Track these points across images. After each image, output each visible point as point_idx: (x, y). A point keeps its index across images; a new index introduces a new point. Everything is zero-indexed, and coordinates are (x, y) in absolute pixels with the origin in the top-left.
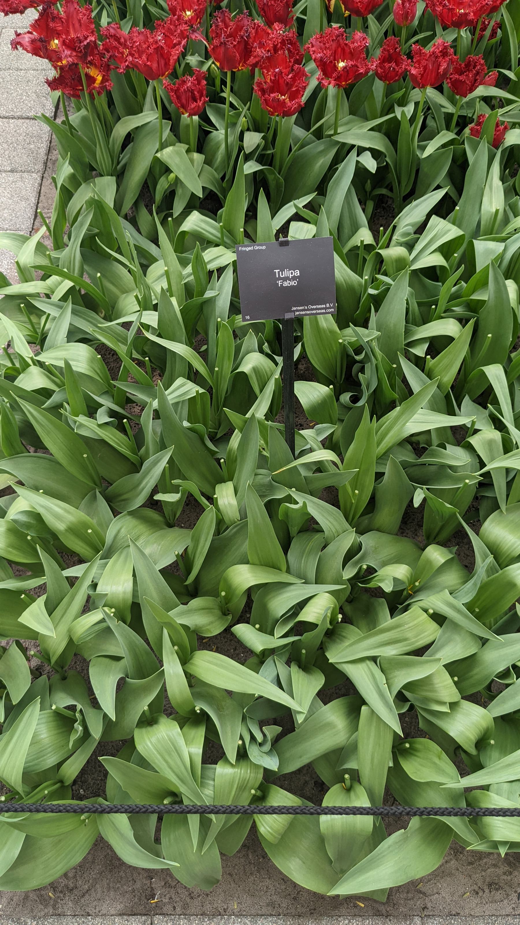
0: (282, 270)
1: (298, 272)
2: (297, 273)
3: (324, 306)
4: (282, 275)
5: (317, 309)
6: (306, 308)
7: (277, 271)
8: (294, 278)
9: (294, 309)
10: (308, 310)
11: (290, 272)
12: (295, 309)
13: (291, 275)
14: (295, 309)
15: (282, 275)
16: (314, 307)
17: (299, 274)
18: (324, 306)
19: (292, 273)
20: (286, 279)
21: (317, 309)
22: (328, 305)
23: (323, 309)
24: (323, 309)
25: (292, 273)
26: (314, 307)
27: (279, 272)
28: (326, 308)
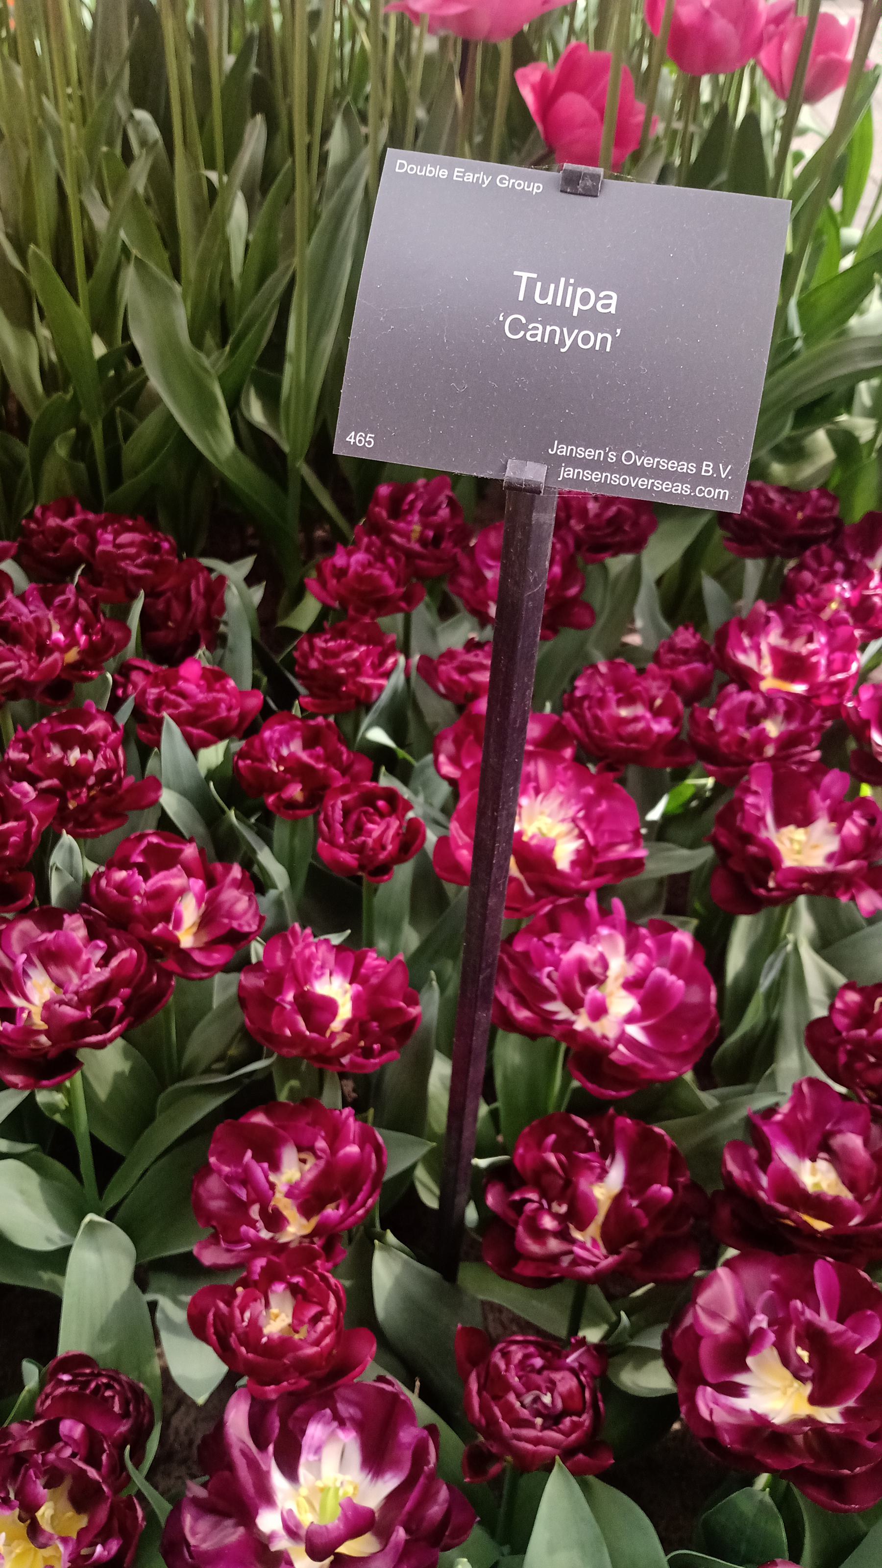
0: (548, 278)
4: (544, 295)
5: (656, 473)
6: (612, 457)
7: (525, 275)
9: (562, 450)
10: (618, 468)
13: (578, 305)
15: (544, 295)
16: (648, 462)
17: (612, 310)
18: (687, 467)
19: (585, 299)
20: (558, 315)
21: (656, 473)
23: (682, 478)
24: (682, 478)
25: (585, 299)
26: (648, 462)
27: (531, 283)
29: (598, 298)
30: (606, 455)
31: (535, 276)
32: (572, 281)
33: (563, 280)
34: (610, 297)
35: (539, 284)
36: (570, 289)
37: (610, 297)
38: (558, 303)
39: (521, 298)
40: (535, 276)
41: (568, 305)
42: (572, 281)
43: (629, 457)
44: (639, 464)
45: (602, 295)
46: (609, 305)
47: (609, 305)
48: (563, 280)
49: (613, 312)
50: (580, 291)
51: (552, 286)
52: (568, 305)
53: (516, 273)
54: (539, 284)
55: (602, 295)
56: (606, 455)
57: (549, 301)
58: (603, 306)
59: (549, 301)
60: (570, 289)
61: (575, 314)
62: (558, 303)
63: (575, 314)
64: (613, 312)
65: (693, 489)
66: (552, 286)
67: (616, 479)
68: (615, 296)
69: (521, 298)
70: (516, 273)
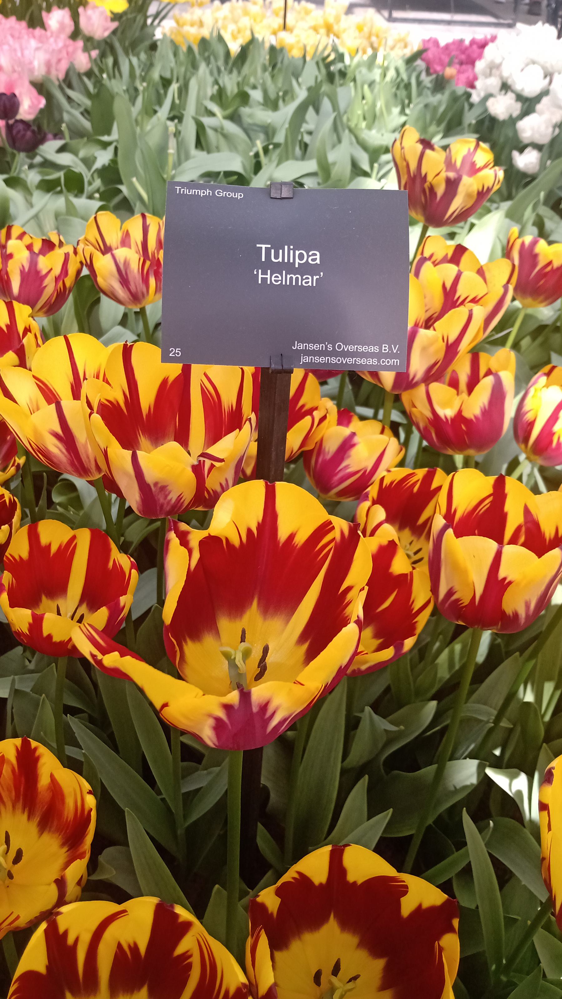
0: (278, 246)
1: (318, 257)
2: (315, 258)
3: (374, 349)
4: (277, 257)
7: (264, 246)
8: (306, 269)
10: (334, 353)
11: (297, 253)
12: (301, 346)
13: (297, 261)
14: (301, 346)
15: (277, 257)
16: (351, 348)
17: (318, 261)
18: (374, 349)
19: (301, 257)
22: (385, 348)
25: (301, 257)
27: (268, 251)
28: (379, 356)
29: (308, 256)
30: (326, 347)
31: (269, 246)
32: (292, 247)
33: (286, 247)
34: (316, 255)
35: (273, 251)
36: (292, 252)
37: (316, 255)
38: (286, 261)
39: (263, 259)
40: (269, 246)
41: (291, 261)
42: (292, 247)
43: (339, 347)
44: (346, 350)
45: (310, 254)
46: (316, 259)
47: (316, 259)
48: (286, 247)
49: (319, 263)
50: (297, 253)
51: (281, 251)
52: (291, 261)
53: (258, 245)
54: (273, 251)
55: (310, 254)
56: (326, 347)
57: (280, 260)
58: (312, 260)
59: (280, 260)
60: (292, 252)
61: (297, 266)
62: (286, 261)
63: (297, 266)
64: (319, 263)
65: (379, 361)
66: (281, 251)
67: (334, 360)
68: (318, 253)
69: (263, 259)
70: (258, 245)
